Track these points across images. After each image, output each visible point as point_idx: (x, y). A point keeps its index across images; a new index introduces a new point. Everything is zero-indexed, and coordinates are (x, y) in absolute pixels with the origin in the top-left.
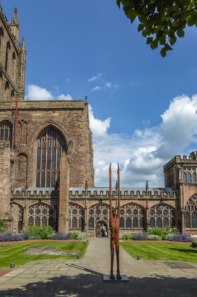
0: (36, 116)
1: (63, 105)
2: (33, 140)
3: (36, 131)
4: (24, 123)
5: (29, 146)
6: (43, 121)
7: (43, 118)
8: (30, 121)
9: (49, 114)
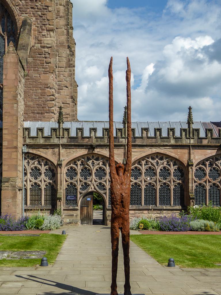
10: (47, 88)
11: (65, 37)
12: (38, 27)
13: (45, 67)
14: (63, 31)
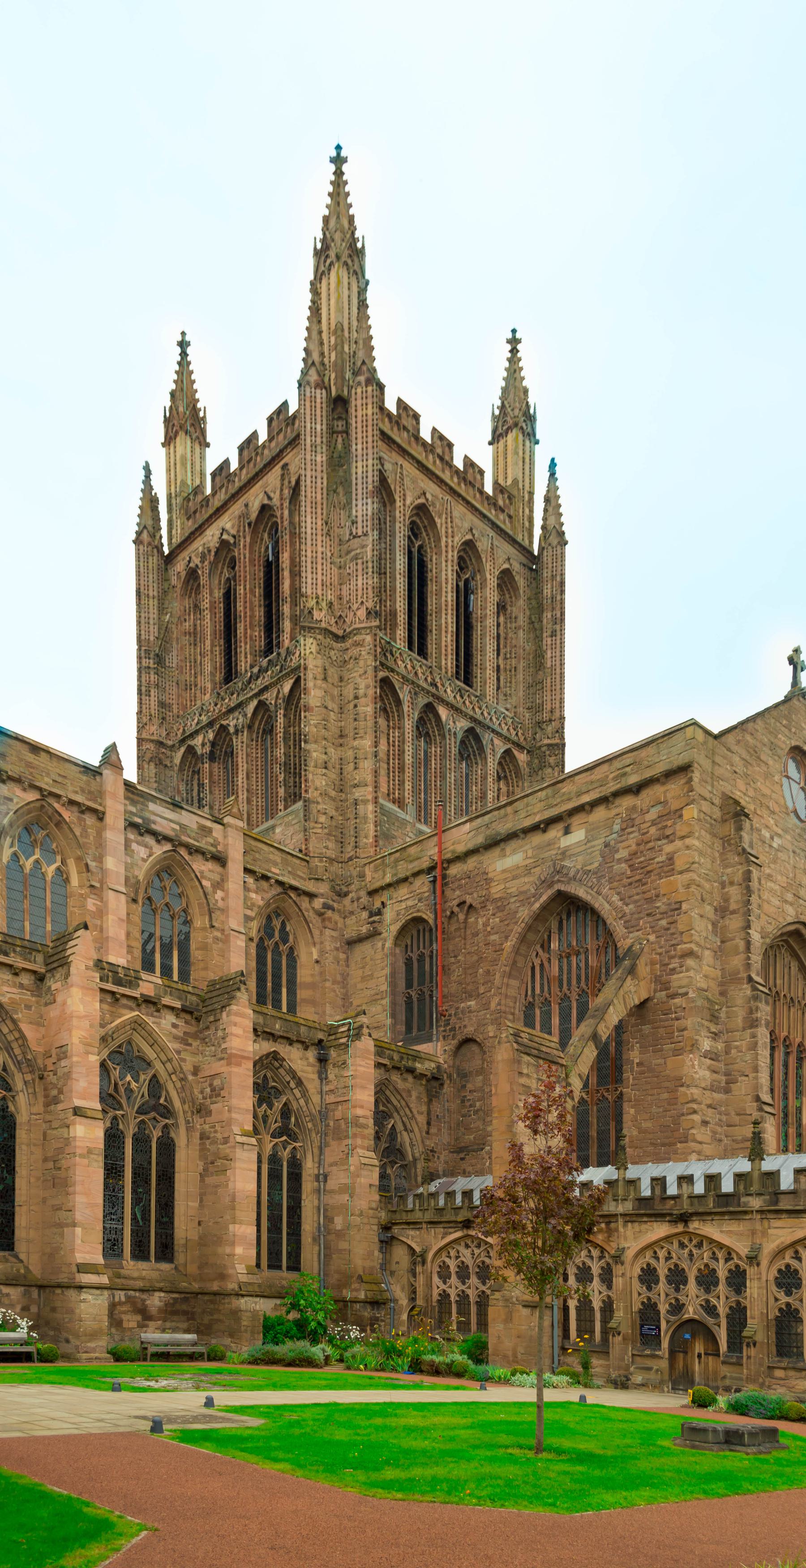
0: (504, 871)
1: (603, 782)
2: (497, 976)
3: (507, 937)
4: (468, 911)
5: (487, 1006)
6: (527, 883)
7: (528, 870)
8: (486, 900)
9: (550, 844)
10: (682, 1086)
11: (743, 956)
12: (660, 954)
13: (676, 1039)
14: (737, 946)
